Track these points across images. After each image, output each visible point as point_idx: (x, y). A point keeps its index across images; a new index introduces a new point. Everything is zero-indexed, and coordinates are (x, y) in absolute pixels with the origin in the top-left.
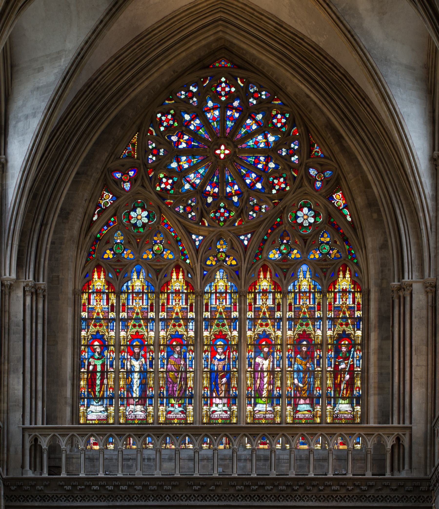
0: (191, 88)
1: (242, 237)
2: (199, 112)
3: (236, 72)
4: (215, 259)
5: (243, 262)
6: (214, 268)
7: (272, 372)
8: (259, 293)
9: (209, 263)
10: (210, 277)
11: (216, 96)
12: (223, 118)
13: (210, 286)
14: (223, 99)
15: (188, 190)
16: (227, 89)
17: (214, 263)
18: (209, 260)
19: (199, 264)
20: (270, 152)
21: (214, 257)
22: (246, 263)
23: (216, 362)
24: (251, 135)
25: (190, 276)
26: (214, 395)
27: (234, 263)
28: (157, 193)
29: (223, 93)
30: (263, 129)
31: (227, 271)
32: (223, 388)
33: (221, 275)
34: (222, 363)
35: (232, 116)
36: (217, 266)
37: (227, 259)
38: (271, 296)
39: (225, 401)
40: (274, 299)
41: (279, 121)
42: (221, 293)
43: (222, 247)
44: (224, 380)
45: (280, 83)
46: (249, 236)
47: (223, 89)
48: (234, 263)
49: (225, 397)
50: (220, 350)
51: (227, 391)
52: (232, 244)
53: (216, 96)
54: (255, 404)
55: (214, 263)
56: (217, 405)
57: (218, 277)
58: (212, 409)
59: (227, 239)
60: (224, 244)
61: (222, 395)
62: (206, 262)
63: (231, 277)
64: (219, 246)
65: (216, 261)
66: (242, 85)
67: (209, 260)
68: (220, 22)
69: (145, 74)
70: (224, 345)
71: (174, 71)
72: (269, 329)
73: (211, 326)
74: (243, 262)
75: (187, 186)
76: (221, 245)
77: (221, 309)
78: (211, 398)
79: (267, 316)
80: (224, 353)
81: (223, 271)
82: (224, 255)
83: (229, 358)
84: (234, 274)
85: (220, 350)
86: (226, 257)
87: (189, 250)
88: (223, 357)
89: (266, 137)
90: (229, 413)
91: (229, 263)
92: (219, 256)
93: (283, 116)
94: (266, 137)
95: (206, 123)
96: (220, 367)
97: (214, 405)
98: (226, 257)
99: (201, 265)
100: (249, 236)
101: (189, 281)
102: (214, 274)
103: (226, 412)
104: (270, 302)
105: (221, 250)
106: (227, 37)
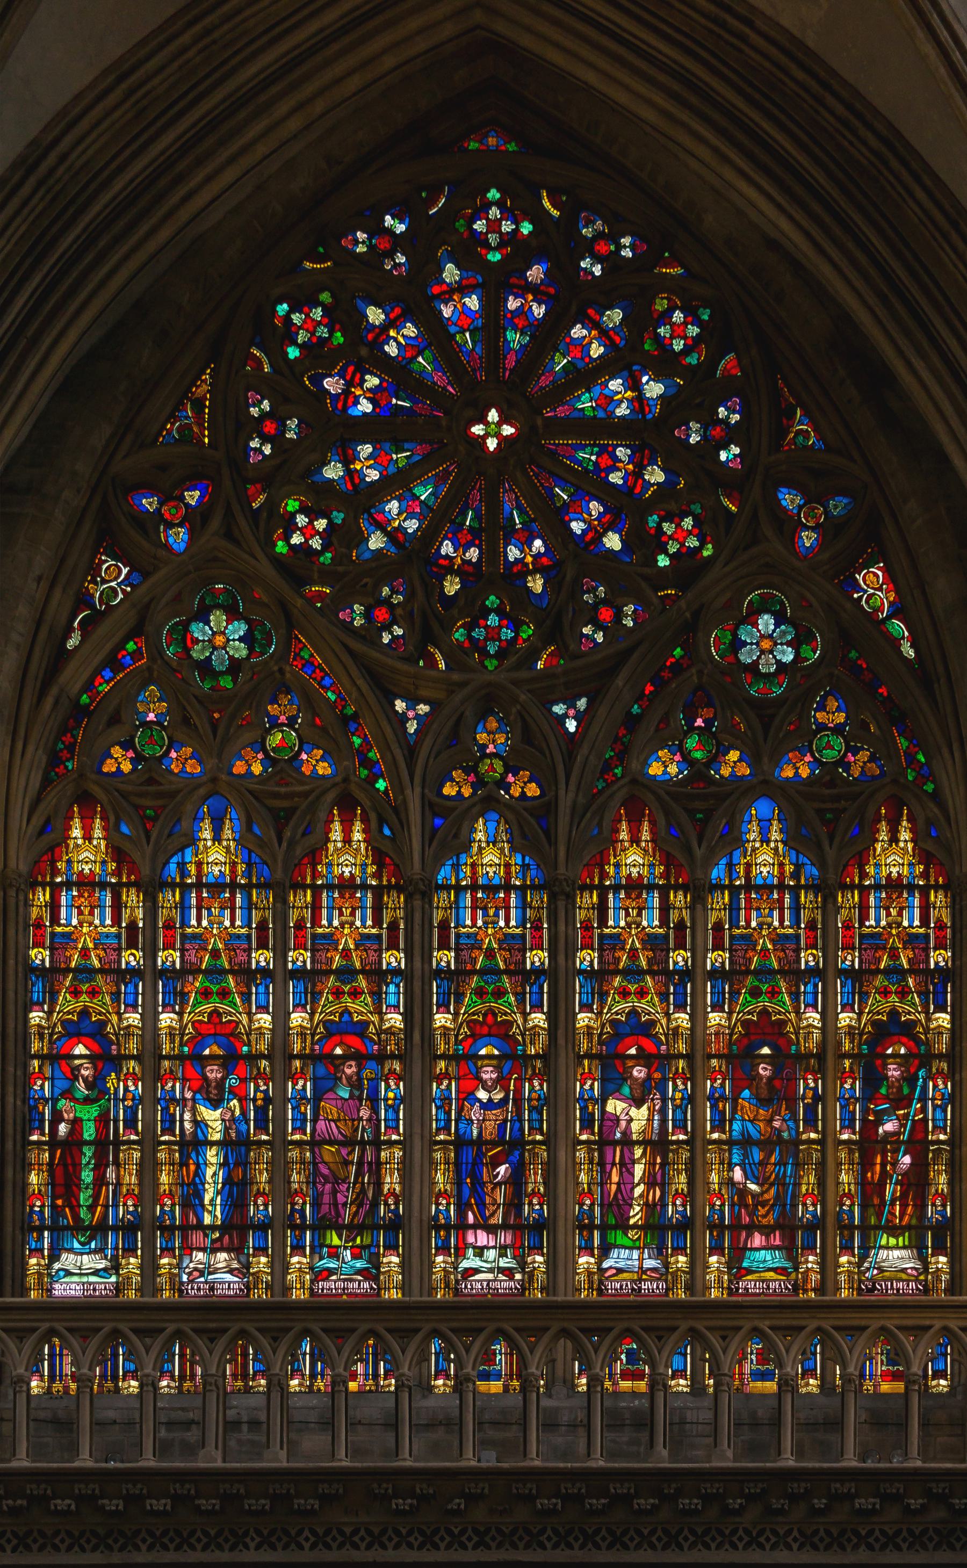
4: (472, 778)
5: (562, 785)
6: (466, 804)
9: (449, 790)
10: (456, 836)
13: (456, 867)
17: (467, 792)
18: (453, 780)
19: (418, 790)
21: (467, 771)
22: (573, 787)
27: (533, 790)
31: (511, 816)
33: (492, 831)
36: (476, 799)
37: (510, 778)
43: (492, 738)
48: (533, 790)
52: (526, 729)
55: (467, 792)
57: (480, 836)
59: (507, 715)
60: (499, 730)
62: (442, 786)
63: (524, 836)
64: (482, 737)
65: (473, 786)
67: (453, 780)
74: (562, 785)
76: (489, 733)
81: (495, 816)
84: (530, 829)
86: (506, 772)
87: (385, 748)
91: (516, 791)
92: (484, 767)
98: (506, 772)
99: (423, 796)
102: (466, 824)
105: (491, 749)
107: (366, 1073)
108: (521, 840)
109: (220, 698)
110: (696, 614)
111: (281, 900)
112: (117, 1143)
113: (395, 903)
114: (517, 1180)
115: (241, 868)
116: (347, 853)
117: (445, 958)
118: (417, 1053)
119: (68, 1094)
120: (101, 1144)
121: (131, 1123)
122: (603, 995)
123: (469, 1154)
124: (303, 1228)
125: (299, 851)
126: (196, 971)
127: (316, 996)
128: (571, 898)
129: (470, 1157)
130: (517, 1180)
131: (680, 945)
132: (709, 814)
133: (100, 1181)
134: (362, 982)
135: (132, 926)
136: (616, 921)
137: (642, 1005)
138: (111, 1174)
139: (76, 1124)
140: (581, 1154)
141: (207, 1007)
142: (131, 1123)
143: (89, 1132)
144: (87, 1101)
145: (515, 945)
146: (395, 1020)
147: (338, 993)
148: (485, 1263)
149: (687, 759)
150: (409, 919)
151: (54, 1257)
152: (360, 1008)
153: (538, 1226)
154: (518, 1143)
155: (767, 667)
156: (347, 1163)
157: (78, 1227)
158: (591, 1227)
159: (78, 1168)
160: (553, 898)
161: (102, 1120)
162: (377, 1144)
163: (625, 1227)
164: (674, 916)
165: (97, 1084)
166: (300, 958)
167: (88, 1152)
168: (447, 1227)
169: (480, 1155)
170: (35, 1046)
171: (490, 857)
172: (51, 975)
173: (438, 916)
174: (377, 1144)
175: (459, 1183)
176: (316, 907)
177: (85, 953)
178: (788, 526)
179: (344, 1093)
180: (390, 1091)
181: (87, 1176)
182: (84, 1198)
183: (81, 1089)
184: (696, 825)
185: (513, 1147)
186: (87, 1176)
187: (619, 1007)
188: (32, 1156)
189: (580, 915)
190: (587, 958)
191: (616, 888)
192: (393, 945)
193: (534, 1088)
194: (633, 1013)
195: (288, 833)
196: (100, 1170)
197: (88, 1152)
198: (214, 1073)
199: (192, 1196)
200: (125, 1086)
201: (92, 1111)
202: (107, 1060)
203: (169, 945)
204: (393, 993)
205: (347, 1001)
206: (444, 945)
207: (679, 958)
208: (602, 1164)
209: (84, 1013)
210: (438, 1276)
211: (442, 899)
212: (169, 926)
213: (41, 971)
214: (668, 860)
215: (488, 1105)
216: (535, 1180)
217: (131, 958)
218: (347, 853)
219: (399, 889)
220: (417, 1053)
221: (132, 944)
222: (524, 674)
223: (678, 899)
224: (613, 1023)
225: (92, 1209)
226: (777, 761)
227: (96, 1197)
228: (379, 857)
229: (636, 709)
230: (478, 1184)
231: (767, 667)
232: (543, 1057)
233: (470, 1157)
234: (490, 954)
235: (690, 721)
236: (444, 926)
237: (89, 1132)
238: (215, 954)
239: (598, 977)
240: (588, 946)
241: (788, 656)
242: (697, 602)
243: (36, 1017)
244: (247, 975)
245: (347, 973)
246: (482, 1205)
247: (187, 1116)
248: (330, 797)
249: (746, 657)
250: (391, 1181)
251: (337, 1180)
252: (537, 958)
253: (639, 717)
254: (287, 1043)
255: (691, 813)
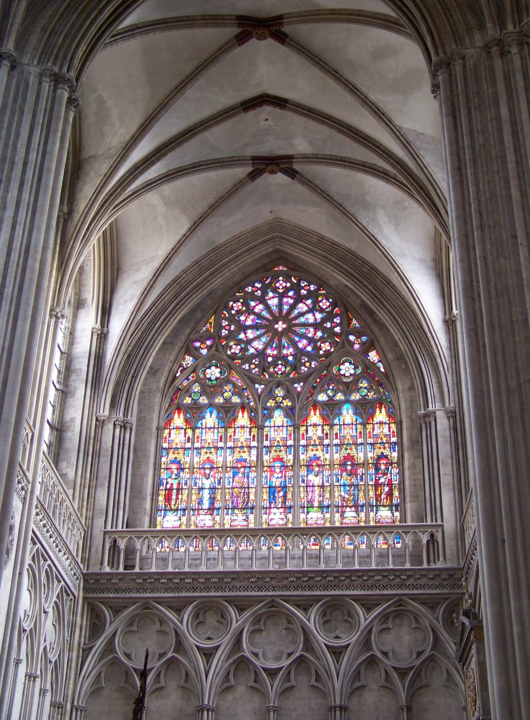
0: (256, 285)
1: (296, 385)
2: (262, 300)
3: (291, 273)
7: (322, 486)
8: (310, 426)
9: (268, 404)
11: (275, 290)
12: (280, 305)
13: (270, 422)
14: (281, 291)
15: (253, 354)
16: (284, 285)
20: (317, 326)
23: (274, 480)
24: (302, 314)
25: (253, 414)
26: (272, 506)
27: (290, 404)
28: (228, 356)
29: (281, 287)
30: (311, 310)
32: (280, 500)
34: (278, 480)
35: (287, 302)
38: (320, 428)
39: (282, 510)
40: (323, 430)
41: (325, 304)
42: (279, 427)
44: (281, 494)
45: (324, 279)
46: (302, 384)
47: (281, 285)
49: (281, 507)
50: (278, 470)
51: (284, 502)
53: (275, 290)
54: (308, 513)
56: (275, 514)
58: (270, 517)
61: (280, 506)
63: (287, 414)
64: (277, 392)
66: (295, 281)
68: (277, 239)
69: (219, 273)
70: (281, 466)
71: (243, 274)
72: (319, 453)
73: (270, 452)
75: (252, 351)
77: (278, 439)
78: (270, 508)
79: (317, 443)
80: (281, 472)
82: (281, 399)
83: (285, 477)
84: (289, 412)
85: (278, 470)
87: (253, 396)
88: (280, 475)
89: (314, 315)
90: (285, 520)
92: (277, 399)
93: (327, 300)
94: (314, 315)
95: (268, 307)
96: (278, 484)
97: (272, 514)
100: (302, 384)
101: (253, 418)
103: (282, 519)
104: (319, 433)
106: (283, 248)
107: (246, 471)
108: (287, 415)
109: (213, 386)
110: (330, 364)
111: (226, 431)
112: (182, 489)
113: (255, 431)
114: (285, 496)
115: (216, 424)
116: (243, 419)
117: (267, 443)
118: (259, 466)
119: (170, 477)
120: (178, 489)
121: (186, 484)
122: (307, 451)
123: (272, 490)
124: (229, 509)
125: (231, 420)
126: (204, 448)
127: (234, 452)
128: (299, 428)
129: (272, 490)
130: (285, 496)
131: (327, 438)
132: (334, 408)
133: (177, 498)
134: (246, 449)
135: (189, 438)
136: (310, 433)
137: (317, 453)
138: (180, 496)
139: (172, 484)
140: (302, 489)
141: (206, 456)
142: (186, 484)
143: (175, 486)
144: (175, 479)
145: (285, 440)
146: (254, 458)
147: (240, 452)
148: (277, 518)
149: (328, 395)
150: (258, 434)
151: (164, 517)
152: (245, 456)
153: (290, 508)
154: (285, 487)
155: (347, 374)
156: (240, 493)
157: (171, 510)
158: (304, 507)
159: (171, 495)
160: (294, 428)
161: (179, 484)
162: (248, 488)
163: (312, 507)
164: (325, 432)
165: (178, 475)
166: (230, 444)
167: (175, 491)
168: (266, 508)
169: (275, 490)
170: (163, 466)
171: (279, 417)
172: (167, 450)
173: (265, 433)
174: (248, 488)
175: (270, 497)
176: (235, 432)
177: (177, 444)
178: (352, 344)
179: (240, 475)
180: (252, 475)
181: (174, 497)
182: (173, 502)
183: (174, 476)
184: (331, 409)
185: (284, 487)
186: (174, 497)
187: (311, 454)
188: (160, 492)
189: (301, 432)
190: (303, 442)
191: (310, 426)
192: (254, 440)
193: (290, 474)
194: (315, 455)
195: (228, 415)
196: (177, 495)
197: (175, 491)
198: (207, 471)
199: (200, 502)
200: (185, 475)
201: (177, 481)
202: (181, 469)
203: (198, 442)
204: (254, 452)
205: (242, 454)
206: (267, 440)
207: (326, 442)
208: (307, 491)
209: (176, 458)
210: (264, 520)
211: (266, 429)
212: (198, 437)
213: (166, 449)
214: (324, 419)
215: (278, 478)
216: (289, 496)
217: (188, 445)
218: (243, 419)
219: (255, 427)
220: (259, 466)
221: (188, 441)
222: (287, 378)
223: (326, 428)
224: (310, 457)
225: (175, 505)
226: (350, 395)
227: (176, 502)
228: (251, 420)
229: (315, 385)
230: (274, 497)
231: (347, 374)
232: (292, 466)
233: (272, 490)
234: (278, 442)
235: (328, 387)
236: (267, 436)
237: (175, 486)
238: (209, 444)
239: (306, 446)
240: (303, 439)
241: (352, 372)
242: (329, 361)
243: (164, 459)
244: (217, 448)
245: (242, 447)
246: (275, 502)
247: (200, 482)
248: (239, 407)
249: (342, 372)
250: (252, 497)
251: (238, 497)
252: (290, 442)
253: (315, 387)
254: (226, 464)
255: (329, 408)
